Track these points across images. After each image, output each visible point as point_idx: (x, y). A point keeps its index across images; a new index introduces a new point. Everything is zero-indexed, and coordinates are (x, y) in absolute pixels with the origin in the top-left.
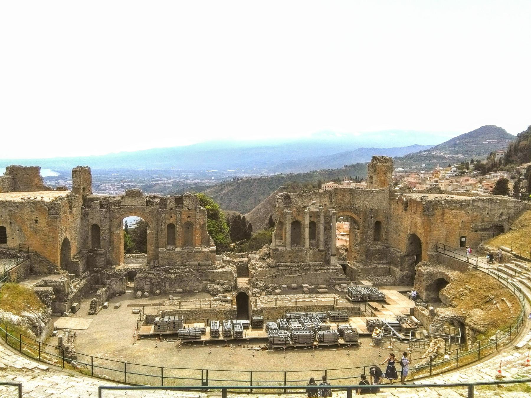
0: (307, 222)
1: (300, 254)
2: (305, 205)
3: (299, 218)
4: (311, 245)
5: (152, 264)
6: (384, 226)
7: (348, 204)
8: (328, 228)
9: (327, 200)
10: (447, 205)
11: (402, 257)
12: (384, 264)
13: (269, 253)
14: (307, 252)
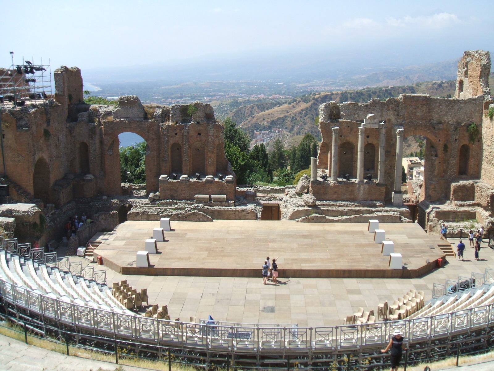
2: (361, 119)
3: (351, 139)
6: (472, 153)
8: (390, 153)
12: (469, 205)
13: (308, 186)
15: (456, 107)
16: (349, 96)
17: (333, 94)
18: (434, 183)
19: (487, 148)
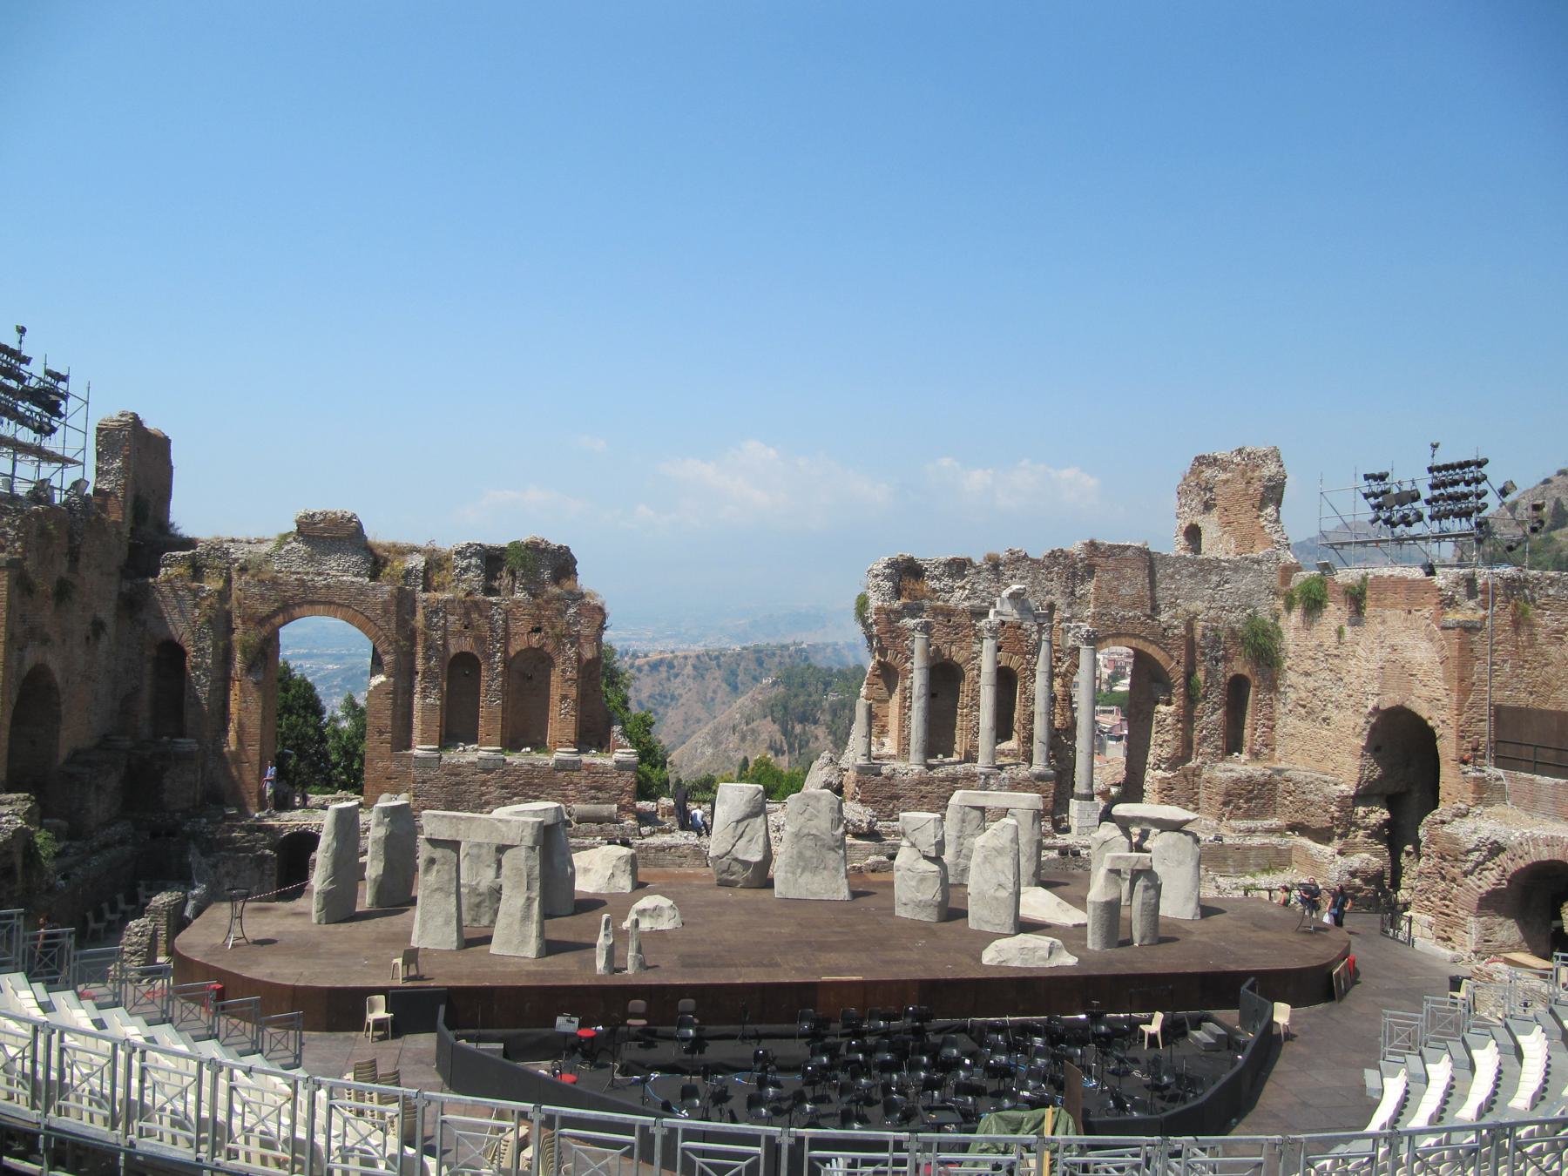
0: (987, 664)
3: (959, 657)
7: (1133, 606)
12: (1270, 831)
19: (1303, 679)
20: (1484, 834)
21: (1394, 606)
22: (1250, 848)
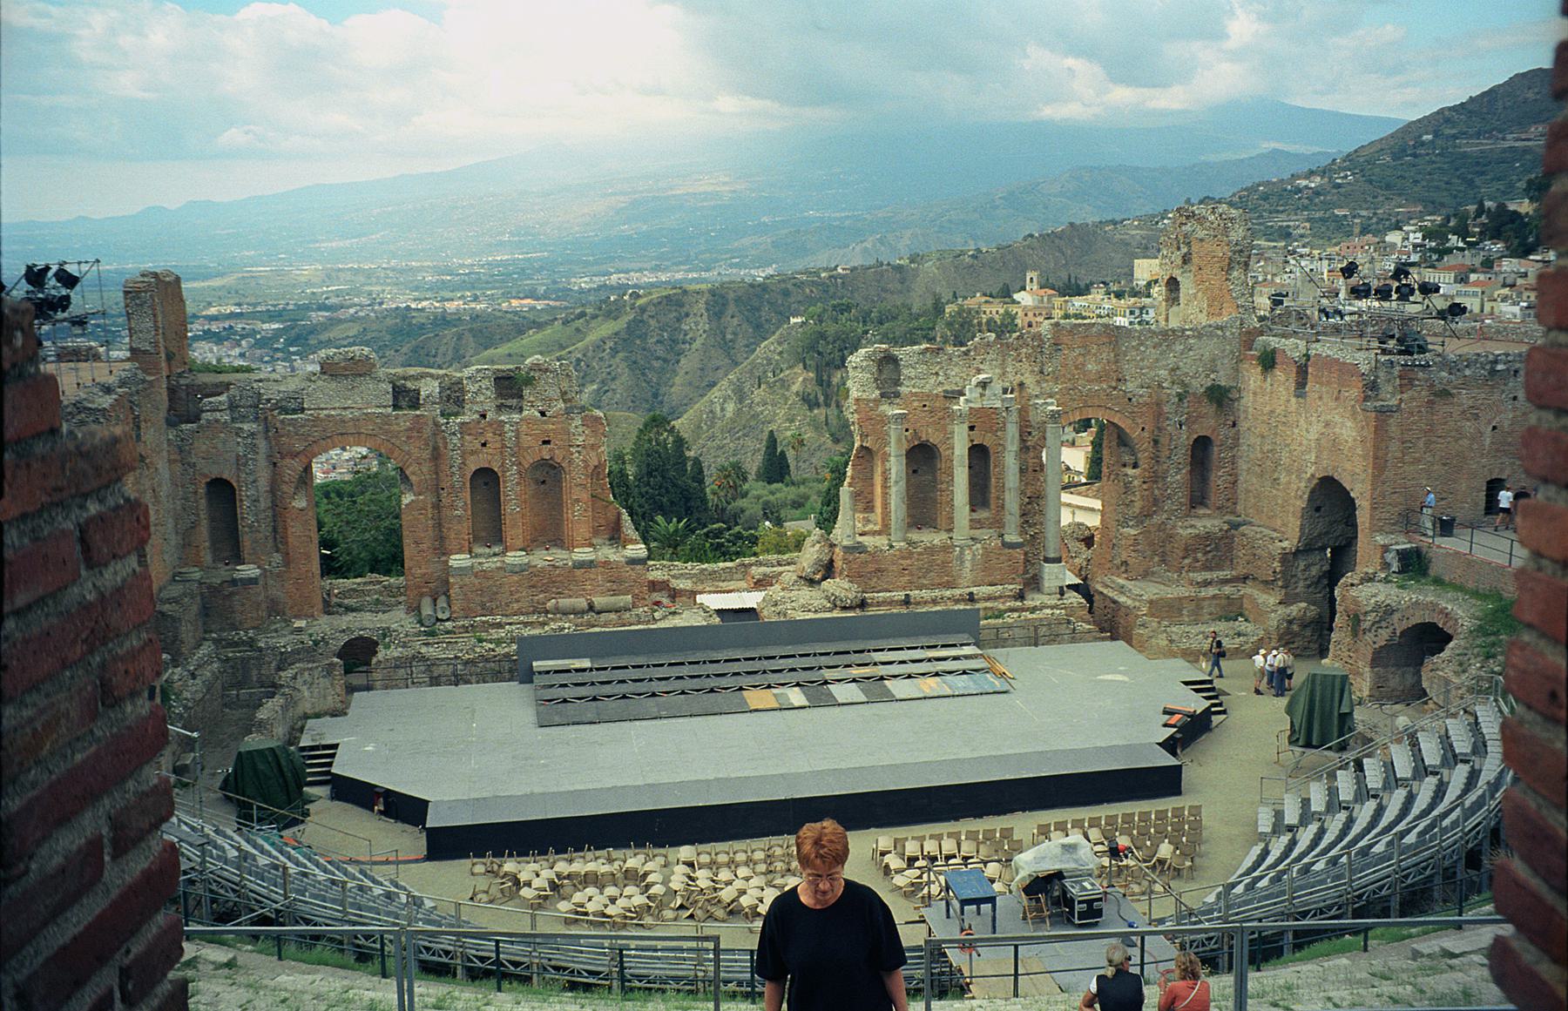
1: (939, 558)
3: (933, 437)
4: (976, 524)
5: (427, 610)
7: (1099, 379)
9: (1026, 365)
10: (1444, 374)
11: (1288, 558)
12: (1225, 582)
13: (831, 561)
14: (962, 553)
15: (1179, 348)
16: (731, 295)
17: (685, 292)
18: (1133, 532)
20: (1381, 598)
21: (1329, 383)
22: (1204, 599)
